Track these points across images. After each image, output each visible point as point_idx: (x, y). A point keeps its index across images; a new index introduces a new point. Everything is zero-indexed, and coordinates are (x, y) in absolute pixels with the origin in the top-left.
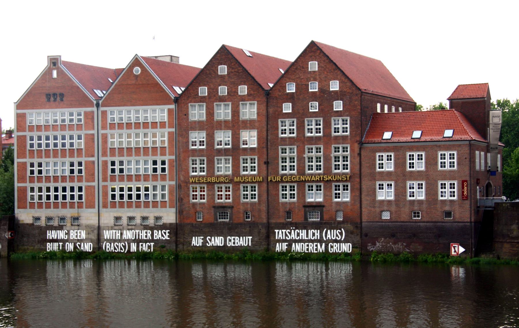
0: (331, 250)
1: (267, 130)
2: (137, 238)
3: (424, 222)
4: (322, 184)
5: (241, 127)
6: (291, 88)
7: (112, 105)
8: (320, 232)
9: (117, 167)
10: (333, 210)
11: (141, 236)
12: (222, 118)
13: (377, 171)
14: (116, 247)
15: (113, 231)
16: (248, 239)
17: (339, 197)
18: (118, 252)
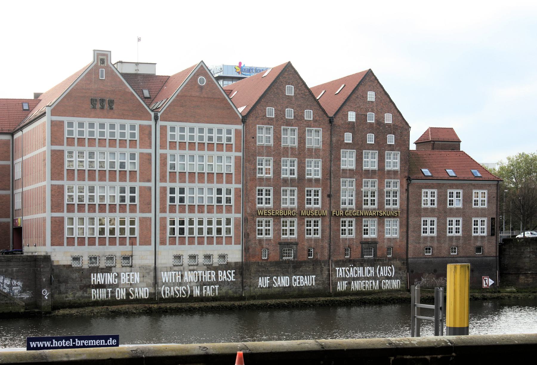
0: (384, 287)
1: (331, 161)
2: (200, 280)
3: (461, 257)
5: (306, 156)
6: (352, 117)
7: (173, 119)
8: (374, 270)
9: (177, 195)
10: (385, 246)
11: (205, 277)
12: (289, 144)
13: (422, 207)
14: (177, 292)
15: (172, 272)
17: (367, 234)
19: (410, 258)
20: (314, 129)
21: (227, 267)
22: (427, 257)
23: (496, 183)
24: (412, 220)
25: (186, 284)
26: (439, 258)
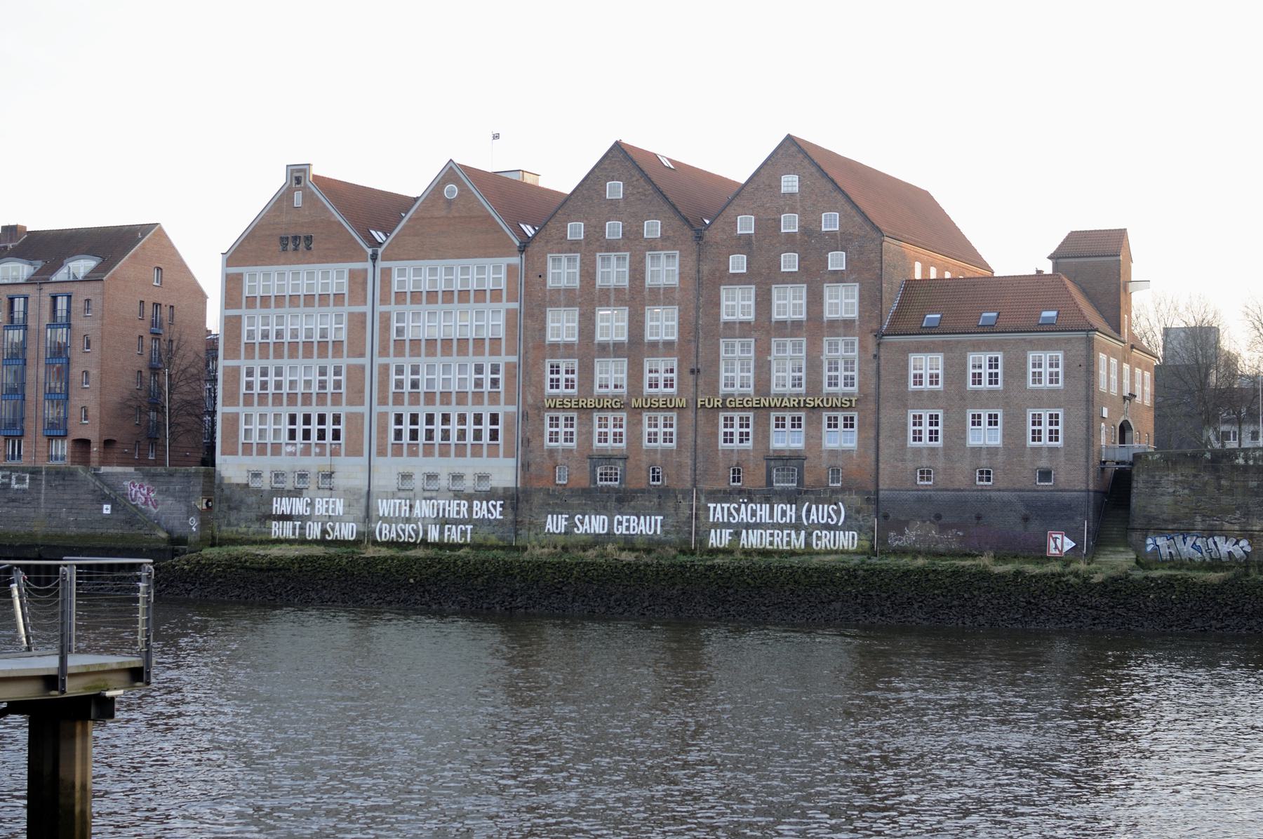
0: (817, 545)
1: (698, 308)
2: (441, 515)
3: (999, 490)
4: (803, 414)
8: (796, 509)
12: (613, 282)
14: (401, 533)
16: (656, 521)
18: (404, 542)
20: (663, 252)
21: (489, 495)
23: (1083, 335)
25: (416, 521)
26: (947, 490)
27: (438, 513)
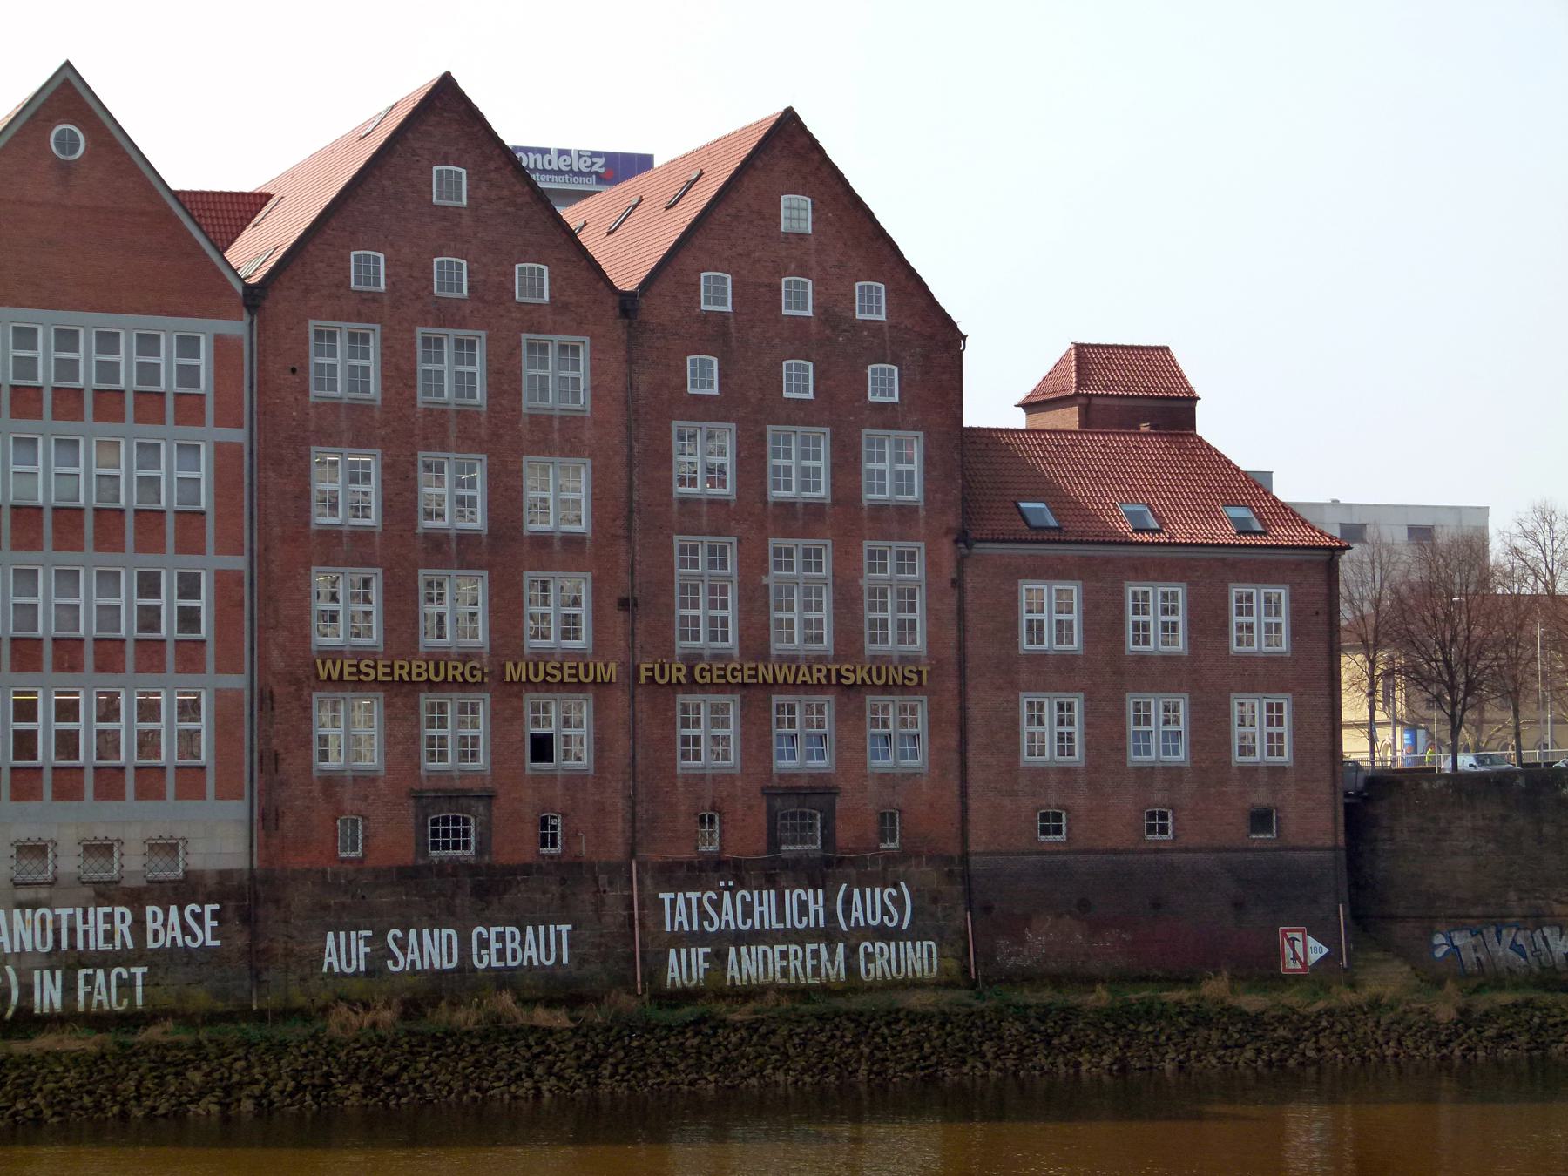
0: (868, 972)
1: (630, 465)
2: (64, 945)
3: (1187, 850)
8: (825, 899)
11: (86, 933)
13: (1021, 652)
16: (558, 935)
19: (976, 854)
20: (557, 338)
21: (182, 891)
22: (1047, 848)
24: (980, 704)
27: (57, 941)
